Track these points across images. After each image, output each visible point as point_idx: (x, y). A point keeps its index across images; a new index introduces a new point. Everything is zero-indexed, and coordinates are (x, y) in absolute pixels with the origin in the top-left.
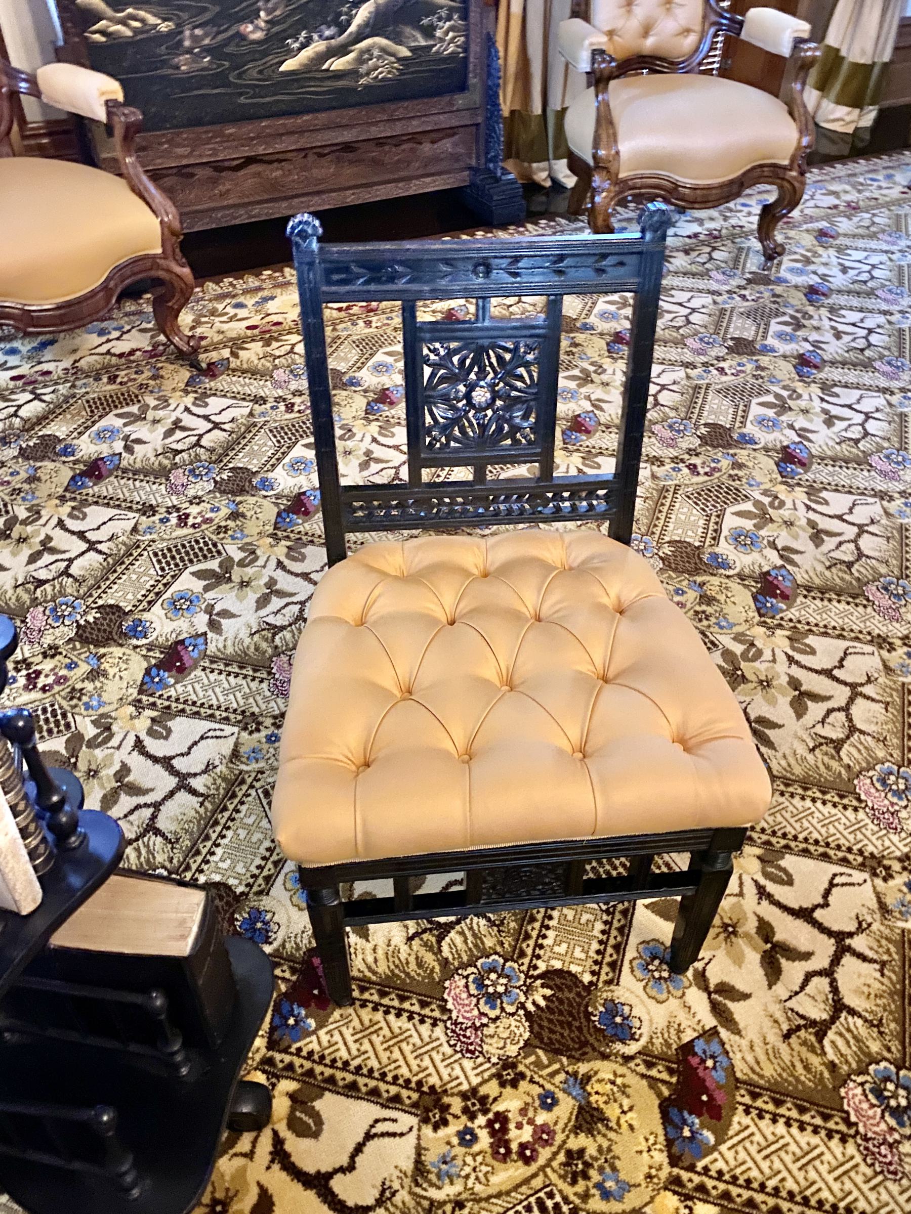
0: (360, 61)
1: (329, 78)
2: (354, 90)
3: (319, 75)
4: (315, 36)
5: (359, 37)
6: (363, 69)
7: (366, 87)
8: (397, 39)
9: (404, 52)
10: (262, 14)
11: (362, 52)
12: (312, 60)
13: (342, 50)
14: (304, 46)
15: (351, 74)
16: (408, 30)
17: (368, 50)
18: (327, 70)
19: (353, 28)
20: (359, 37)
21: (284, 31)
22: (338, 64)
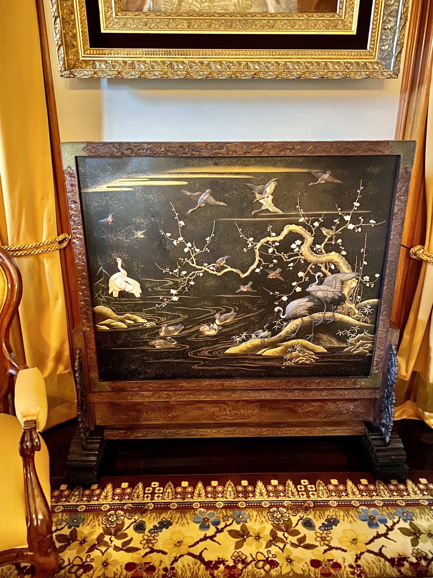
0: (285, 351)
1: (260, 360)
2: (280, 368)
3: (254, 357)
4: (253, 335)
5: (285, 339)
6: (288, 356)
7: (287, 367)
8: (317, 341)
9: (321, 349)
10: (217, 321)
11: (287, 347)
12: (249, 349)
13: (273, 345)
14: (244, 341)
15: (280, 359)
16: (325, 337)
17: (293, 347)
18: (260, 355)
19: (282, 333)
20: (285, 339)
21: (233, 331)
22: (269, 352)
